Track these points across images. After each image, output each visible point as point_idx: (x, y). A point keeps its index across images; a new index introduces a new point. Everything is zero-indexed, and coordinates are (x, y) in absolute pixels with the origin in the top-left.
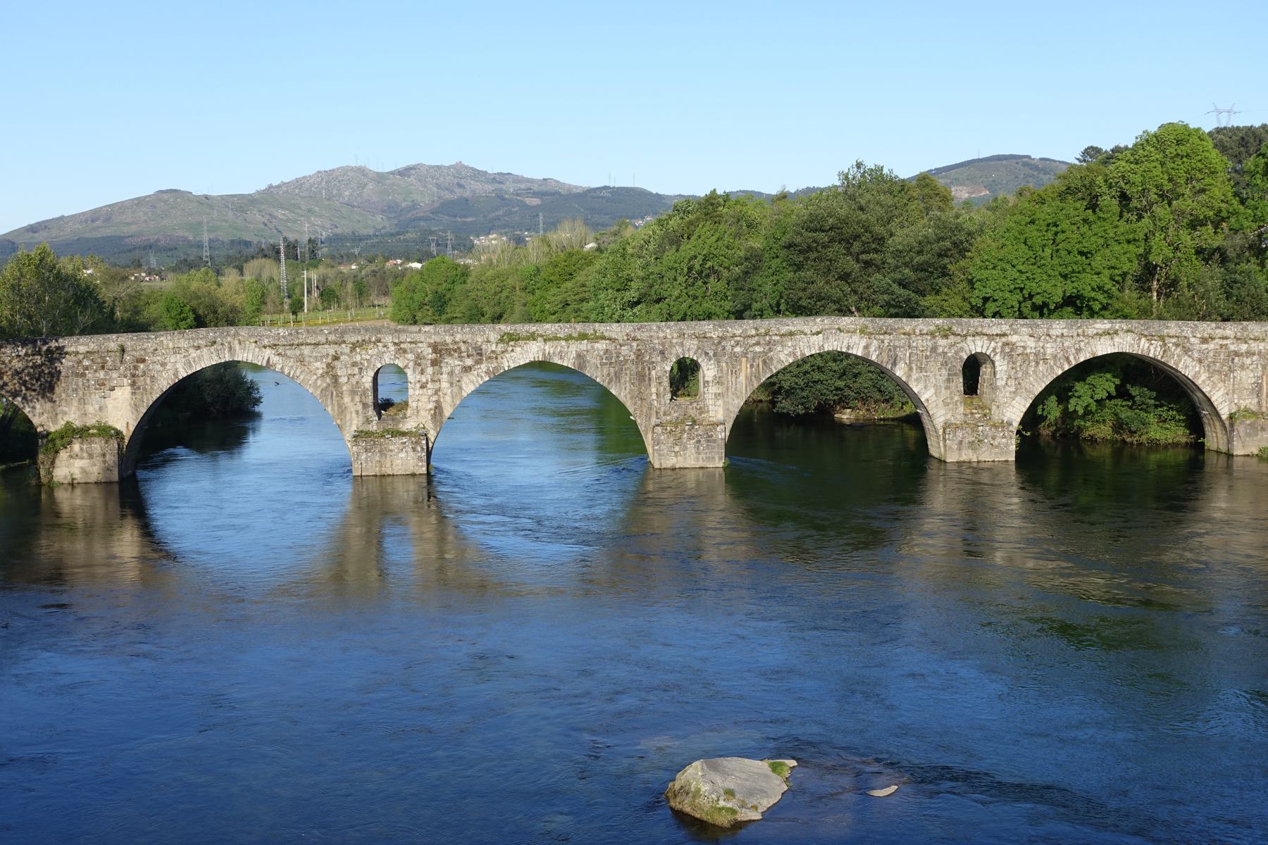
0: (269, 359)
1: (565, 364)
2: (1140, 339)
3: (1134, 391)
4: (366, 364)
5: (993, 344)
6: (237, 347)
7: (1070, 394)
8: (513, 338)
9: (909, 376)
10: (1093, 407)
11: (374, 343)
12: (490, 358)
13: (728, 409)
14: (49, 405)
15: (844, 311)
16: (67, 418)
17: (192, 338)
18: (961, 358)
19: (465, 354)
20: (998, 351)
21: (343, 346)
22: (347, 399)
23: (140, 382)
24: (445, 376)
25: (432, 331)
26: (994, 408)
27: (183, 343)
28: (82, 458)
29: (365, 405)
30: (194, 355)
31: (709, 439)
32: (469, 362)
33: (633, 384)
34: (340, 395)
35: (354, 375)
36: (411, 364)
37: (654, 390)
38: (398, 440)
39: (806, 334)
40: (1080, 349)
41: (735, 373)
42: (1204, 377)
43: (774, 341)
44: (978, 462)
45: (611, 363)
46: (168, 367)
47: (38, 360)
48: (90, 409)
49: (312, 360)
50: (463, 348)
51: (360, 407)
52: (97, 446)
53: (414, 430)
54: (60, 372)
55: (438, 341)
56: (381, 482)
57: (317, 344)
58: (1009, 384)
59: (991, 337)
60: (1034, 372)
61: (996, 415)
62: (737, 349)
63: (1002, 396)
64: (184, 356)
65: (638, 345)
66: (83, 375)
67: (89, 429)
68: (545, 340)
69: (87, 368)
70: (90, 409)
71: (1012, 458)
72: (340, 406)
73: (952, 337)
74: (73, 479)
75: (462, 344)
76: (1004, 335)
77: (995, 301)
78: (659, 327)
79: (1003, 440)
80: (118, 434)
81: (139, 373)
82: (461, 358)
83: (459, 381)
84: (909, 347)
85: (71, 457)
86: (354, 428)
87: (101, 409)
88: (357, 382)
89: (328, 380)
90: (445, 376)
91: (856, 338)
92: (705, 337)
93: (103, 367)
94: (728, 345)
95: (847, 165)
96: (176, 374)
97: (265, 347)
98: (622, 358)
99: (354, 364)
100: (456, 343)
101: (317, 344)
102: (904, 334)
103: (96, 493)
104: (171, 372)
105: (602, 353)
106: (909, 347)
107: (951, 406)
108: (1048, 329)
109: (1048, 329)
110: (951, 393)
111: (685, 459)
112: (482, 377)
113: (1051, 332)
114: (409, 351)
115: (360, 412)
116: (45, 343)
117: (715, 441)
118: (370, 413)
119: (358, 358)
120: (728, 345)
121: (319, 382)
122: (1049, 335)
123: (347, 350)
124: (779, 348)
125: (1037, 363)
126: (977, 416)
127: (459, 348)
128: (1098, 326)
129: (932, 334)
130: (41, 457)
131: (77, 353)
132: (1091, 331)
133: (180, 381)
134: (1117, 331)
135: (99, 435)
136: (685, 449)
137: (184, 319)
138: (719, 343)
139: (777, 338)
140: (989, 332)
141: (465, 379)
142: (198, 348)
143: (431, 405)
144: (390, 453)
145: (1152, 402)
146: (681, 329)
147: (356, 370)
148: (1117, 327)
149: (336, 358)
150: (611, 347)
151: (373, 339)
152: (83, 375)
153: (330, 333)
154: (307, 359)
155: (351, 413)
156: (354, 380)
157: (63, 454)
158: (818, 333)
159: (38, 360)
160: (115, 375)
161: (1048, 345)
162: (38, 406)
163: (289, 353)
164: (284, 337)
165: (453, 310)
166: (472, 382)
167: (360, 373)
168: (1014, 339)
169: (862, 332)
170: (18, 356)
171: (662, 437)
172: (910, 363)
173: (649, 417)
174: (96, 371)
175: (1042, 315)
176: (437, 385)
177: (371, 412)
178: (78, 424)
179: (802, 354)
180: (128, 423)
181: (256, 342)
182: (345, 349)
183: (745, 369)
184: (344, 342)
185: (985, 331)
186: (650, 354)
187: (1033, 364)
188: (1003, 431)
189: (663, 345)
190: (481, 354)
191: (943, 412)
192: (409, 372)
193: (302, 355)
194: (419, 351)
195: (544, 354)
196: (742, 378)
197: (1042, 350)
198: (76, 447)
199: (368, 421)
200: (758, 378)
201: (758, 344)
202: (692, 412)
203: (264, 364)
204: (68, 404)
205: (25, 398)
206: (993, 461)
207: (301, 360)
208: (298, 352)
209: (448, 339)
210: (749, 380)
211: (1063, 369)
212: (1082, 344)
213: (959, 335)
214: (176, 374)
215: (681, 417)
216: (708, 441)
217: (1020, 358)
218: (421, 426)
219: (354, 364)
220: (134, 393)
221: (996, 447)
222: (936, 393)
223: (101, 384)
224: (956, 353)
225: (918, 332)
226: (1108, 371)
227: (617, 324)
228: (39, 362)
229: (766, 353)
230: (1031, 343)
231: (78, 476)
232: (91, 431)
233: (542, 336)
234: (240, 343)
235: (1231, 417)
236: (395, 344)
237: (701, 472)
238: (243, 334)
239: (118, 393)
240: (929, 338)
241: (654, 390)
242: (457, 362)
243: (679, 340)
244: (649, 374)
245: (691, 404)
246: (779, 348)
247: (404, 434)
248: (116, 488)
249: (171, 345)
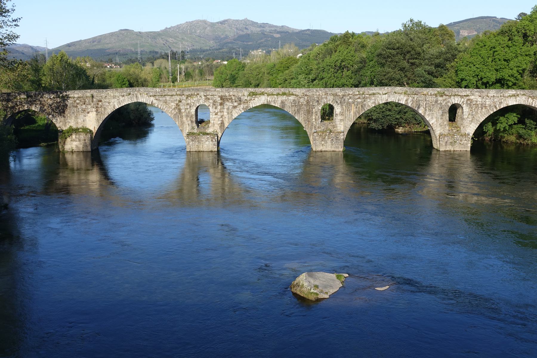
0: (152, 101)
1: (276, 106)
2: (528, 98)
3: (527, 121)
4: (192, 104)
5: (463, 100)
7: (497, 122)
8: (254, 94)
9: (425, 113)
10: (507, 128)
11: (196, 95)
12: (244, 102)
13: (345, 126)
14: (63, 119)
15: (401, 85)
16: (70, 125)
17: (121, 92)
18: (448, 105)
19: (234, 101)
20: (464, 103)
21: (183, 96)
22: (184, 119)
23: (100, 110)
24: (225, 110)
25: (220, 90)
26: (462, 127)
27: (117, 94)
28: (76, 141)
29: (192, 122)
30: (121, 99)
31: (337, 138)
32: (236, 104)
33: (305, 114)
34: (182, 117)
35: (188, 109)
36: (211, 104)
37: (314, 117)
38: (206, 137)
39: (380, 94)
40: (501, 102)
41: (349, 111)
43: (366, 97)
44: (454, 151)
45: (296, 106)
46: (111, 104)
47: (59, 100)
48: (79, 121)
49: (170, 102)
50: (233, 98)
51: (190, 122)
52: (82, 136)
53: (212, 132)
54: (67, 105)
55: (223, 95)
56: (198, 155)
57: (172, 95)
58: (469, 117)
59: (462, 97)
60: (481, 112)
61: (463, 131)
62: (350, 100)
63: (466, 123)
64: (118, 100)
65: (307, 98)
66: (76, 107)
67: (79, 129)
68: (268, 95)
69: (78, 104)
70: (79, 121)
71: (469, 149)
72: (181, 122)
73: (445, 96)
74: (73, 150)
75: (233, 97)
76: (468, 96)
77: (466, 80)
78: (317, 91)
79: (465, 142)
80: (91, 131)
81: (99, 106)
82: (232, 102)
83: (231, 112)
84: (425, 100)
85: (71, 140)
86: (187, 131)
87: (84, 121)
88: (189, 112)
89: (177, 111)
90: (225, 110)
91: (402, 96)
92: (336, 95)
93: (84, 104)
94: (346, 98)
95: (406, 20)
96: (114, 107)
97: (151, 96)
98: (300, 104)
99: (188, 104)
100: (230, 96)
101: (172, 95)
102: (423, 95)
103: (82, 156)
104: (112, 106)
105: (292, 101)
106: (425, 100)
107: (443, 126)
108: (488, 93)
109: (488, 93)
110: (443, 121)
111: (326, 147)
112: (241, 110)
113: (489, 95)
114: (210, 99)
115: (190, 124)
116: (61, 93)
117: (339, 140)
118: (194, 125)
119: (189, 102)
120: (346, 98)
121: (173, 112)
122: (487, 96)
123: (185, 98)
124: (369, 100)
125: (482, 108)
126: (454, 131)
127: (232, 98)
128: (510, 92)
129: (436, 95)
130: (60, 140)
131: (74, 97)
132: (507, 95)
133: (116, 110)
134: (518, 94)
135: (83, 132)
136: (327, 143)
137: (124, 84)
138: (343, 97)
139: (368, 96)
140: (461, 94)
142: (123, 96)
143: (220, 122)
145: (534, 126)
146: (326, 91)
147: (188, 107)
148: (518, 93)
149: (180, 101)
150: (296, 99)
151: (196, 94)
152: (76, 107)
153: (178, 91)
154: (168, 102)
156: (187, 111)
157: (69, 139)
158: (386, 94)
159: (59, 100)
160: (89, 107)
161: (487, 101)
162: (58, 119)
163: (160, 99)
164: (158, 92)
165: (239, 82)
166: (237, 112)
167: (190, 108)
168: (472, 97)
169: (405, 93)
170: (50, 98)
171: (317, 138)
172: (426, 107)
173: (311, 129)
174: (82, 105)
175: (486, 87)
176: (222, 114)
177: (194, 125)
178: (74, 127)
179: (378, 103)
180: (95, 127)
181: (147, 94)
182: (184, 97)
183: (353, 109)
184: (183, 95)
185: (459, 94)
186: (313, 102)
187: (480, 108)
188: (465, 137)
189: (318, 98)
190: (241, 101)
191: (439, 129)
192: (210, 108)
193: (166, 100)
194: (215, 99)
195: (267, 101)
196: (352, 113)
197: (484, 103)
198: (74, 136)
199: (193, 128)
200: (359, 113)
201: (359, 98)
202: (330, 127)
203: (150, 104)
204: (71, 119)
205: (53, 115)
206: (461, 151)
207: (166, 102)
208: (164, 99)
209: (227, 94)
210: (355, 113)
211: (493, 110)
212: (502, 100)
213: (448, 95)
214: (114, 107)
215: (325, 129)
216: (336, 140)
217: (474, 106)
218: (215, 131)
219: (188, 104)
220: (97, 115)
221: (462, 144)
222: (436, 121)
224: (446, 103)
225: (429, 94)
226: (515, 112)
227: (299, 89)
228: (59, 101)
229: (363, 102)
230: (480, 99)
231: (75, 149)
232: (80, 130)
233: (267, 93)
234: (140, 94)
236: (205, 96)
237: (333, 152)
240: (434, 96)
241: (314, 117)
242: (231, 104)
243: (325, 96)
244: (312, 110)
245: (330, 123)
246: (369, 100)
247: (208, 134)
248: (90, 154)
249: (112, 95)
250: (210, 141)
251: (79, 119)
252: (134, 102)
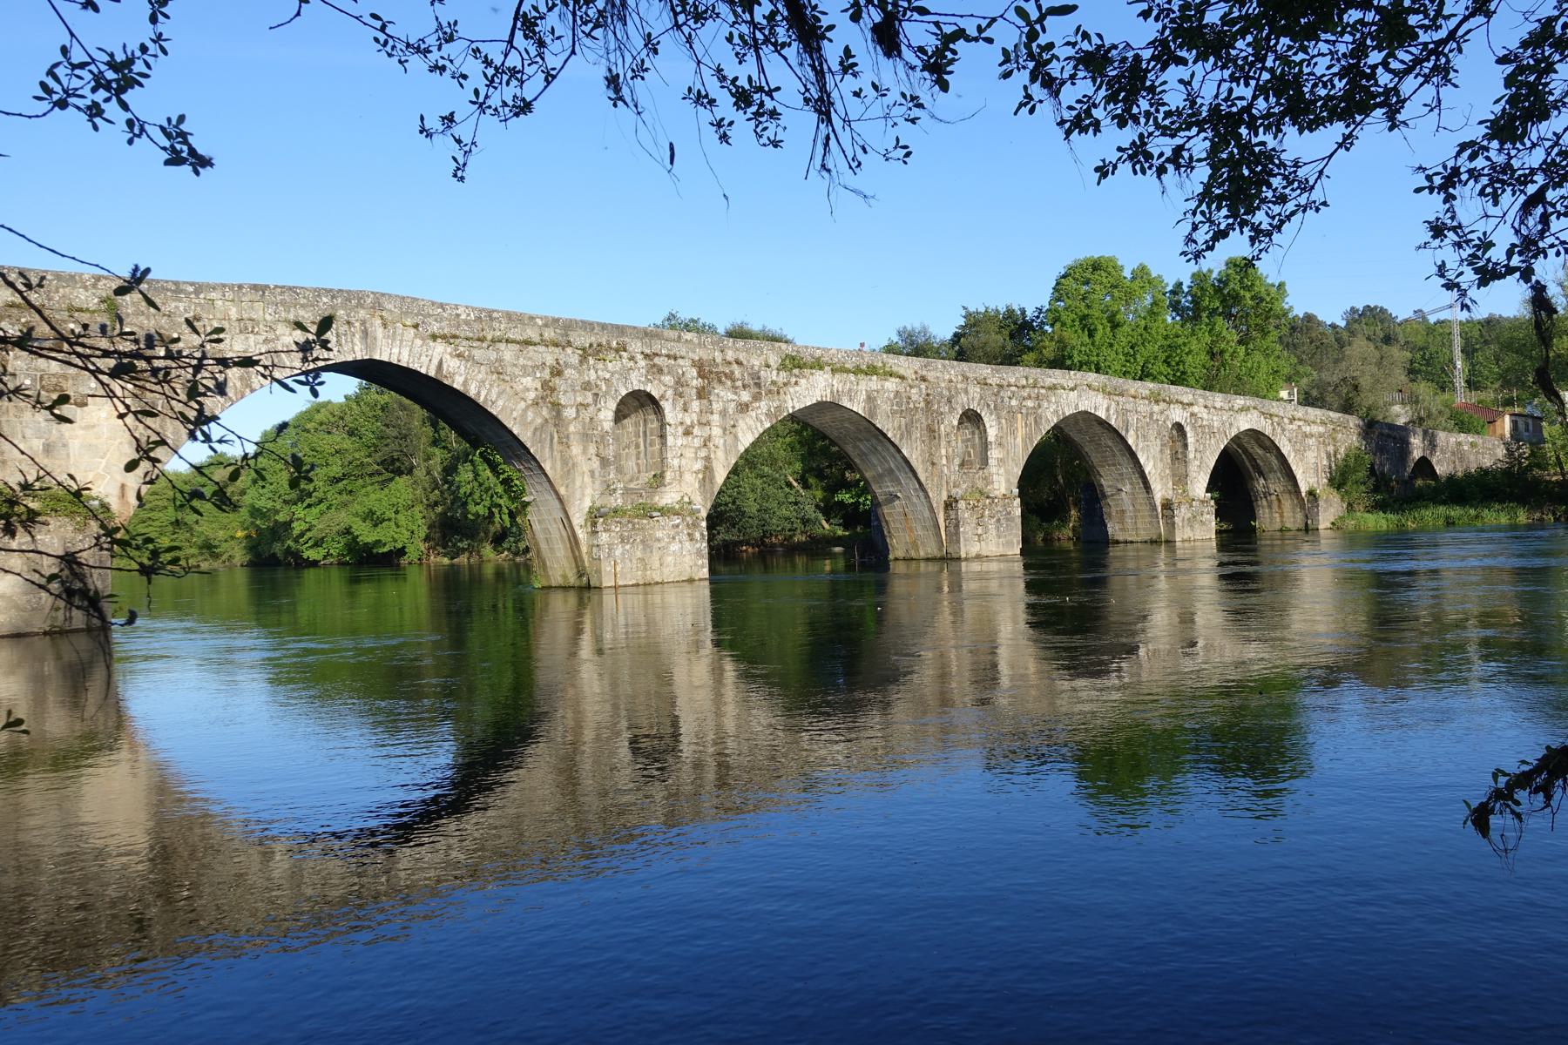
1: (855, 409)
4: (604, 388)
6: (380, 332)
11: (617, 351)
17: (283, 303)
19: (739, 383)
21: (569, 350)
24: (716, 418)
25: (696, 340)
32: (745, 396)
34: (565, 442)
35: (588, 405)
36: (670, 393)
37: (943, 452)
41: (1013, 433)
42: (1293, 454)
49: (517, 371)
51: (596, 463)
55: (705, 357)
57: (528, 343)
62: (1014, 402)
64: (266, 341)
72: (565, 461)
75: (735, 366)
83: (734, 426)
86: (587, 503)
89: (545, 412)
97: (434, 337)
98: (911, 406)
101: (528, 343)
105: (892, 396)
112: (761, 422)
114: (666, 370)
115: (597, 474)
118: (612, 476)
121: (530, 415)
123: (575, 360)
127: (732, 373)
139: (1043, 391)
141: (741, 424)
143: (699, 465)
144: (658, 545)
149: (557, 372)
158: (1072, 389)
163: (477, 354)
164: (467, 323)
166: (750, 428)
167: (595, 402)
168: (1195, 409)
176: (706, 431)
180: (123, 486)
181: (416, 326)
184: (569, 344)
185: (1181, 398)
186: (939, 403)
190: (758, 385)
192: (666, 406)
193: (500, 360)
195: (832, 392)
196: (1019, 440)
201: (1030, 397)
202: (980, 484)
207: (498, 371)
208: (493, 356)
209: (719, 357)
218: (686, 499)
219: (587, 386)
234: (385, 325)
235: (1311, 493)
236: (646, 356)
238: (390, 307)
241: (943, 452)
242: (731, 396)
243: (964, 386)
250: (685, 538)
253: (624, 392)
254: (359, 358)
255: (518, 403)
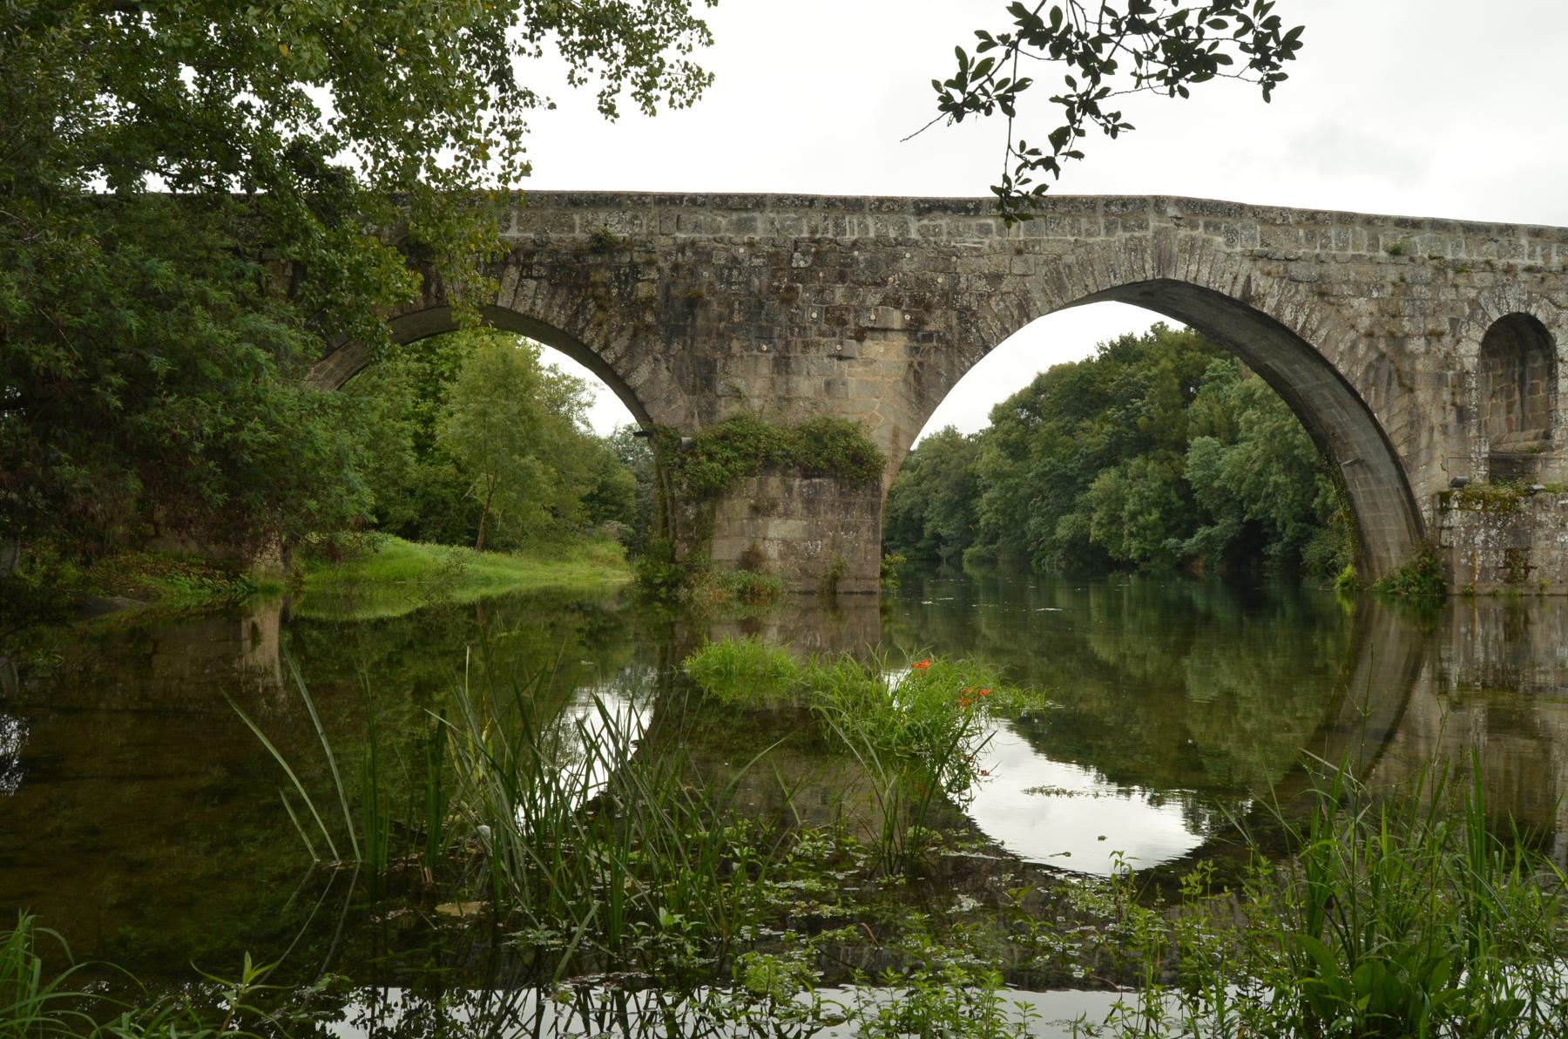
0: (1249, 278)
28: (787, 514)
49: (1346, 290)
51: (1452, 417)
70: (805, 386)
88: (1447, 355)
115: (1451, 429)
121: (1362, 349)
155: (1432, 429)
160: (873, 298)
203: (1237, 295)
220: (915, 350)
223: (836, 319)
239: (873, 348)
251: (799, 373)
252: (1146, 282)
253: (1496, 316)
254: (1150, 278)
255: (1346, 332)
